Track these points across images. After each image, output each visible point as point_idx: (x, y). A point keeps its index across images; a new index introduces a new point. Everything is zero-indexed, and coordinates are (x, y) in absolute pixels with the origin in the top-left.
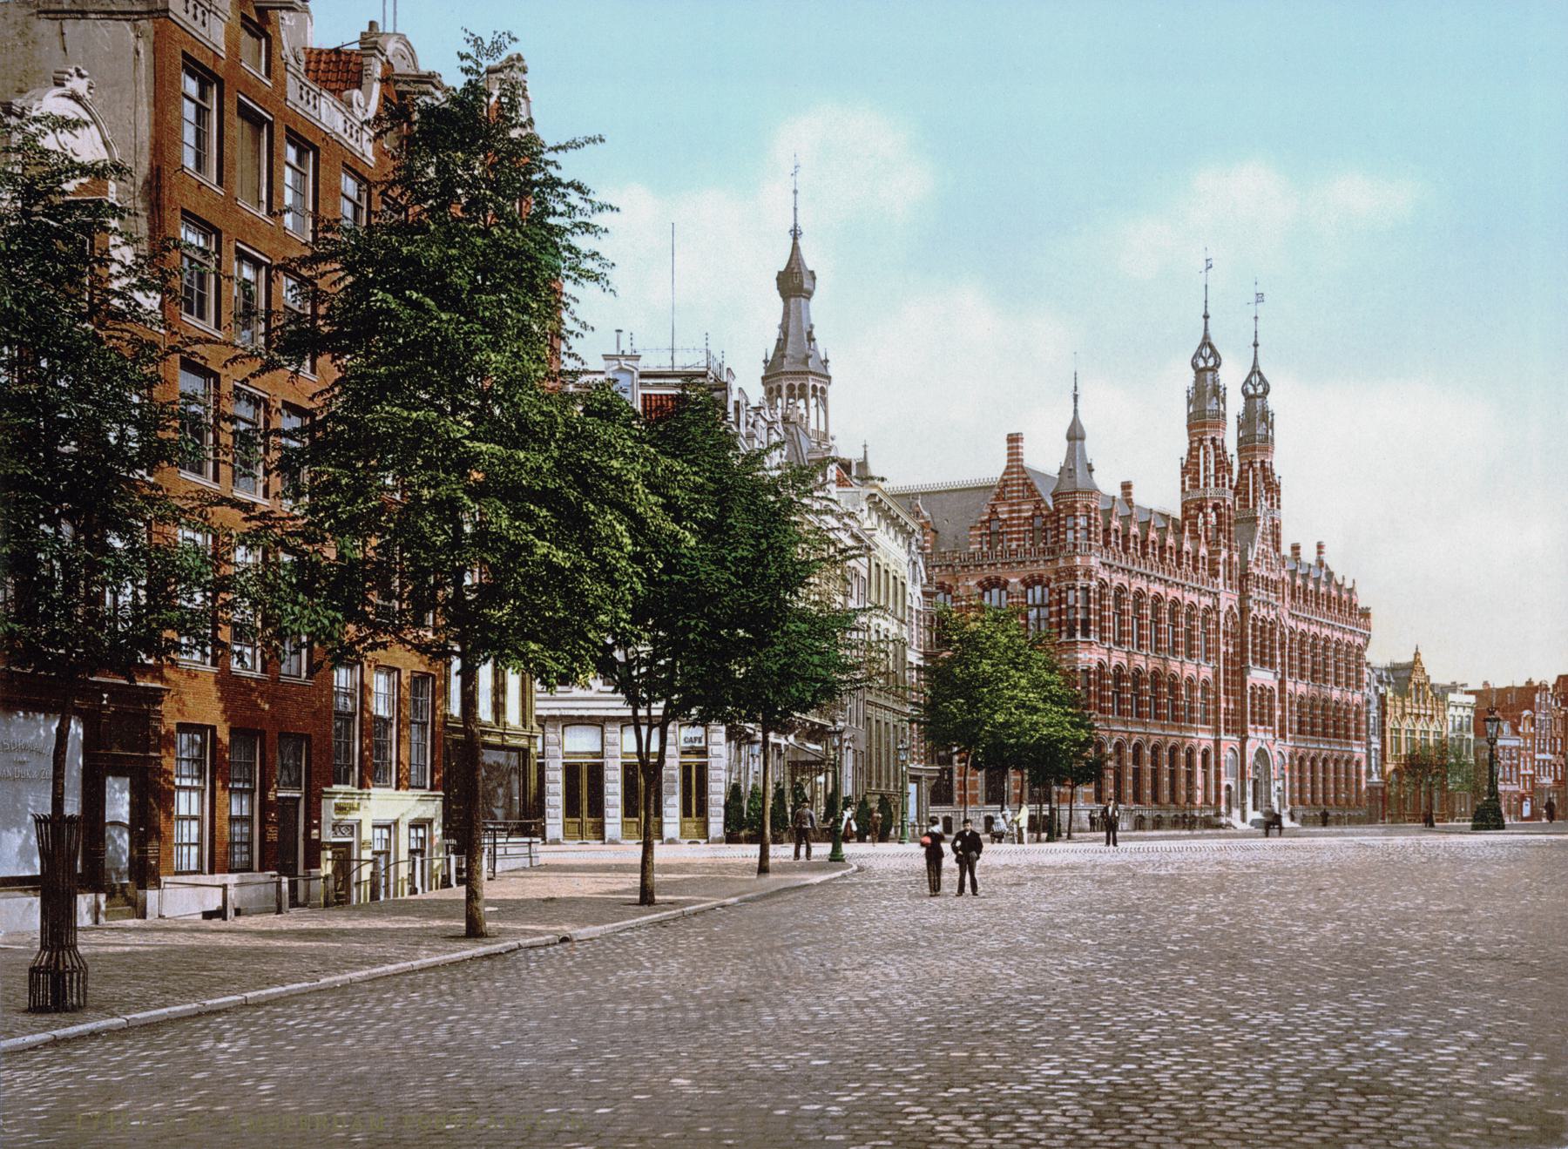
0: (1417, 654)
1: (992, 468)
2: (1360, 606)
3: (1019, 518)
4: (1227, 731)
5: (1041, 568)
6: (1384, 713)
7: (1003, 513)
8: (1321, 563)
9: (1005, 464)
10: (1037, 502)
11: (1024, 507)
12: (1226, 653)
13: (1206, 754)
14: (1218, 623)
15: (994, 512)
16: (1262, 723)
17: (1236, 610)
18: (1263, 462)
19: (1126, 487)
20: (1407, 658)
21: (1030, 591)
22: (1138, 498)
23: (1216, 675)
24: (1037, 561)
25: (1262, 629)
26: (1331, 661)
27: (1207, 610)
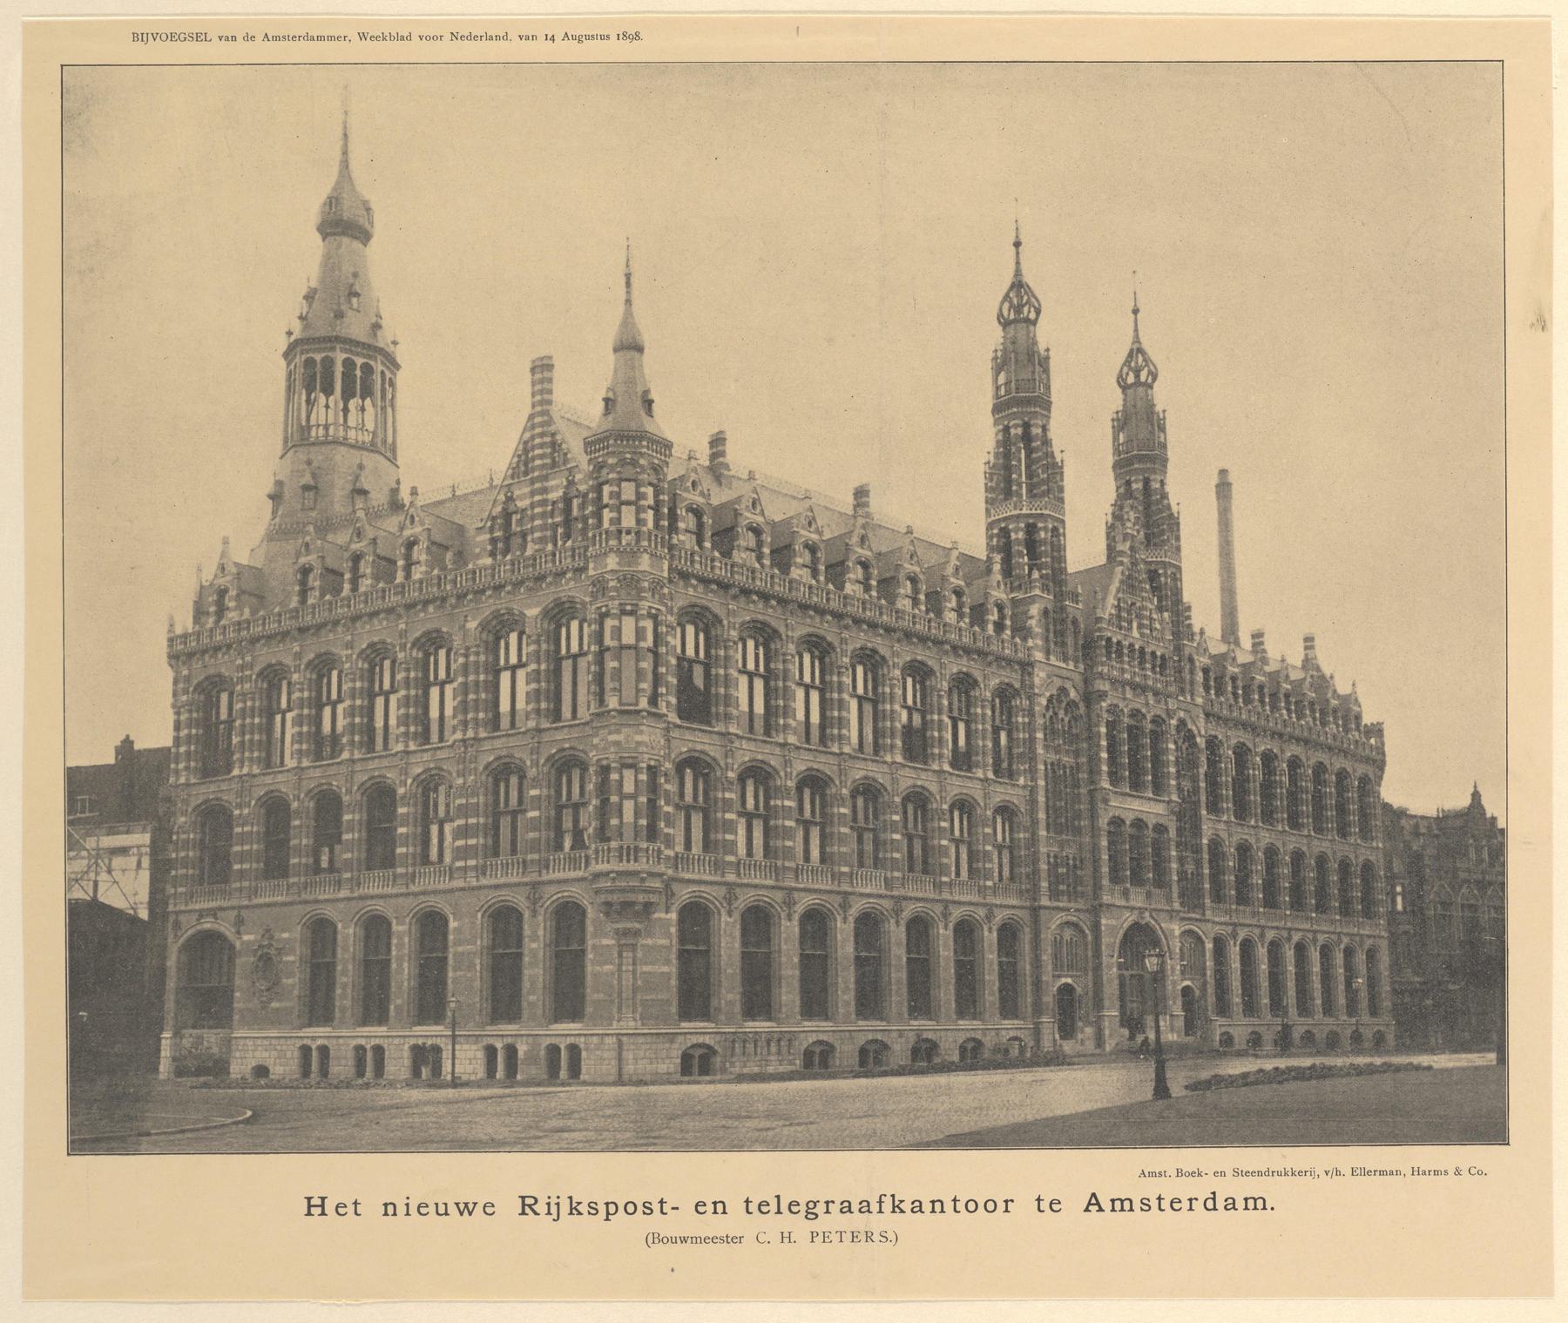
0: (1476, 795)
2: (1367, 719)
3: (544, 503)
4: (1054, 894)
6: (1422, 881)
7: (521, 498)
8: (1308, 663)
9: (528, 410)
10: (570, 470)
11: (552, 483)
12: (1053, 767)
13: (1008, 934)
14: (1031, 713)
15: (510, 499)
16: (1137, 880)
18: (1147, 482)
20: (1464, 802)
22: (875, 503)
25: (1134, 732)
26: (1353, 807)
27: (1005, 694)
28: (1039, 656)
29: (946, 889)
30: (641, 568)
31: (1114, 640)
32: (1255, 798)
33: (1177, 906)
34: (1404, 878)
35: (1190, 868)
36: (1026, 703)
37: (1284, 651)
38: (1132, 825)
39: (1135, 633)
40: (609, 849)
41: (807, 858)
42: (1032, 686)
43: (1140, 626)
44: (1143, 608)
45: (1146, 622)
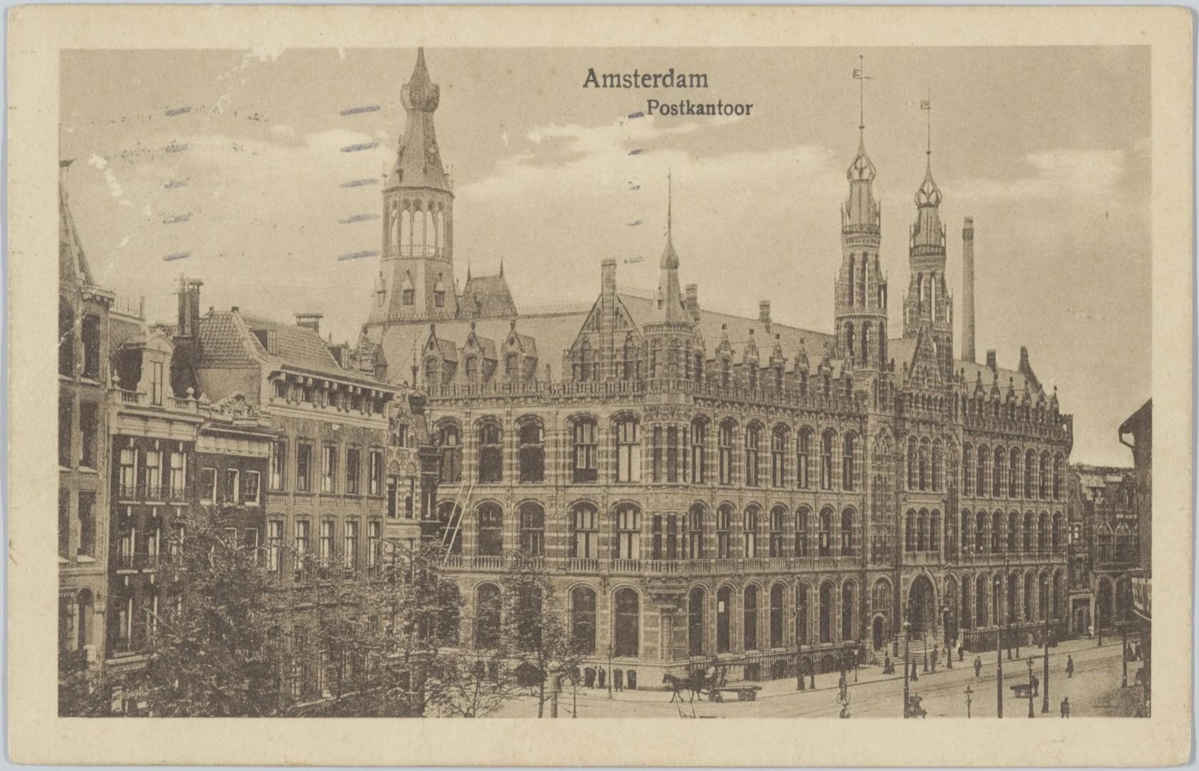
1: (588, 294)
5: (627, 406)
14: (865, 448)
17: (889, 430)
19: (765, 306)
21: (621, 428)
22: (776, 316)
23: (863, 504)
24: (627, 397)
28: (870, 410)
29: (816, 564)
30: (681, 403)
31: (914, 394)
32: (990, 481)
33: (943, 562)
34: (1081, 521)
35: (950, 533)
36: (862, 441)
37: (1009, 361)
38: (920, 512)
39: (926, 387)
40: (660, 564)
41: (747, 556)
42: (866, 431)
43: (929, 381)
44: (932, 368)
45: (933, 378)
